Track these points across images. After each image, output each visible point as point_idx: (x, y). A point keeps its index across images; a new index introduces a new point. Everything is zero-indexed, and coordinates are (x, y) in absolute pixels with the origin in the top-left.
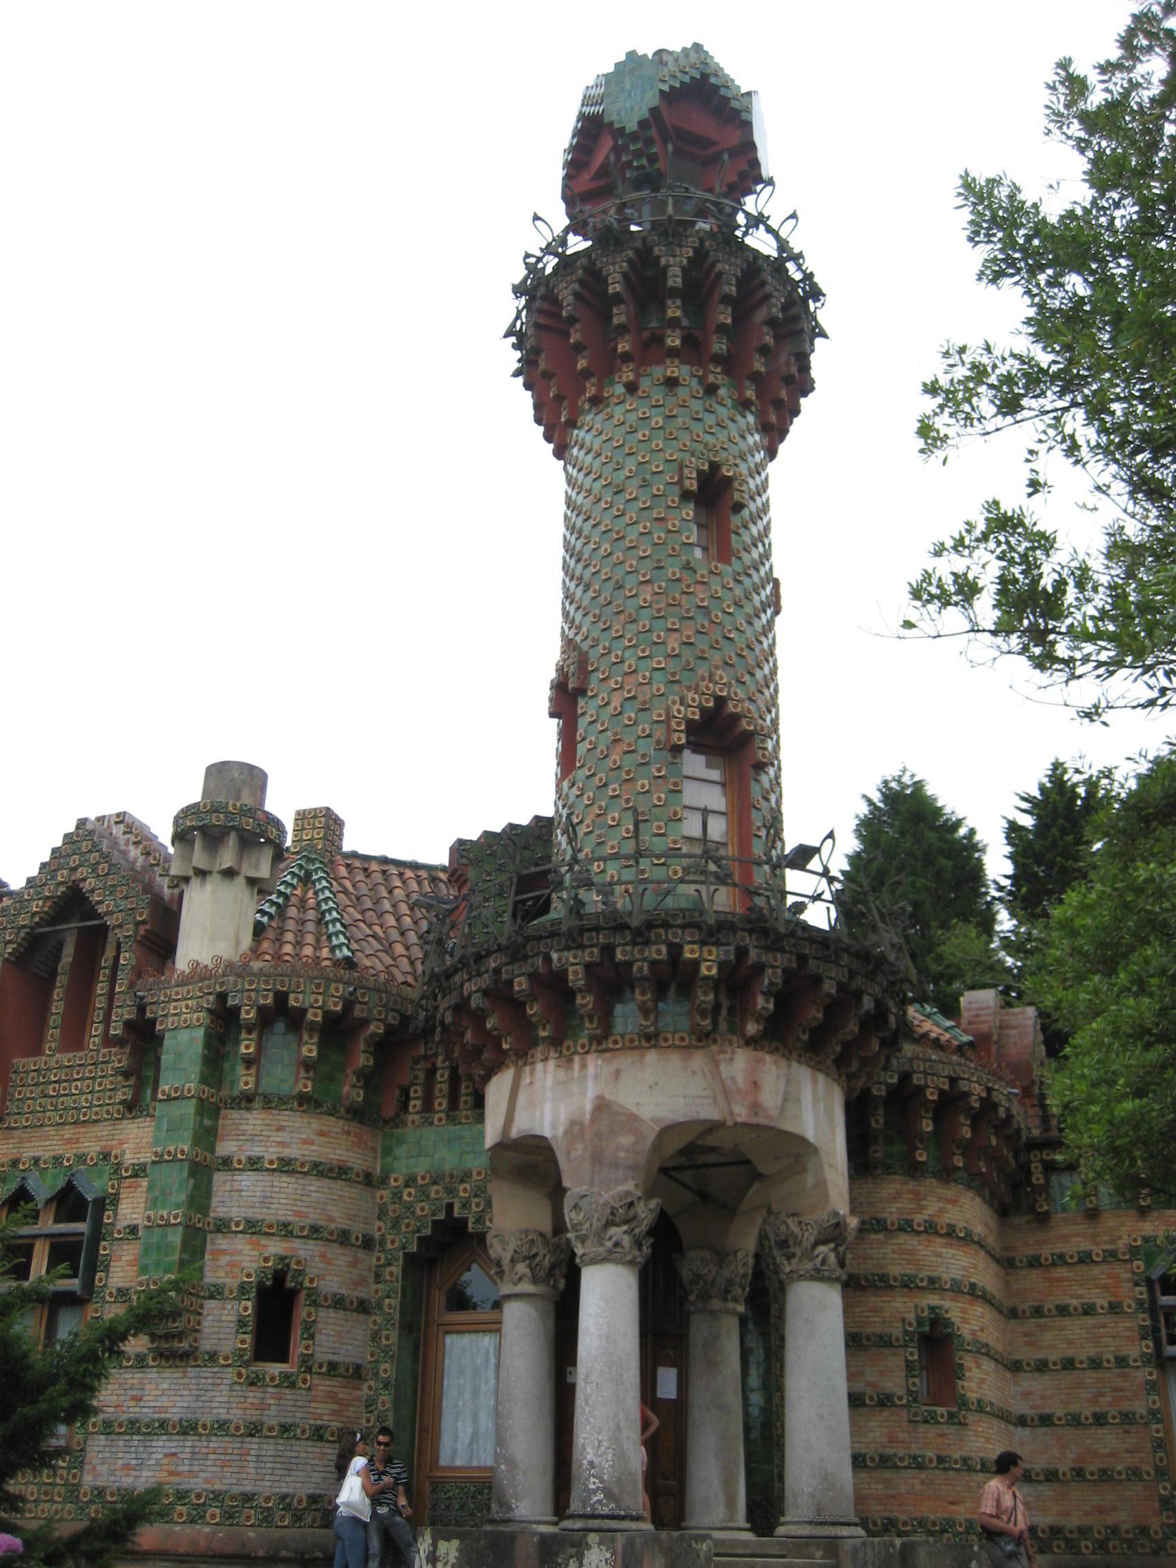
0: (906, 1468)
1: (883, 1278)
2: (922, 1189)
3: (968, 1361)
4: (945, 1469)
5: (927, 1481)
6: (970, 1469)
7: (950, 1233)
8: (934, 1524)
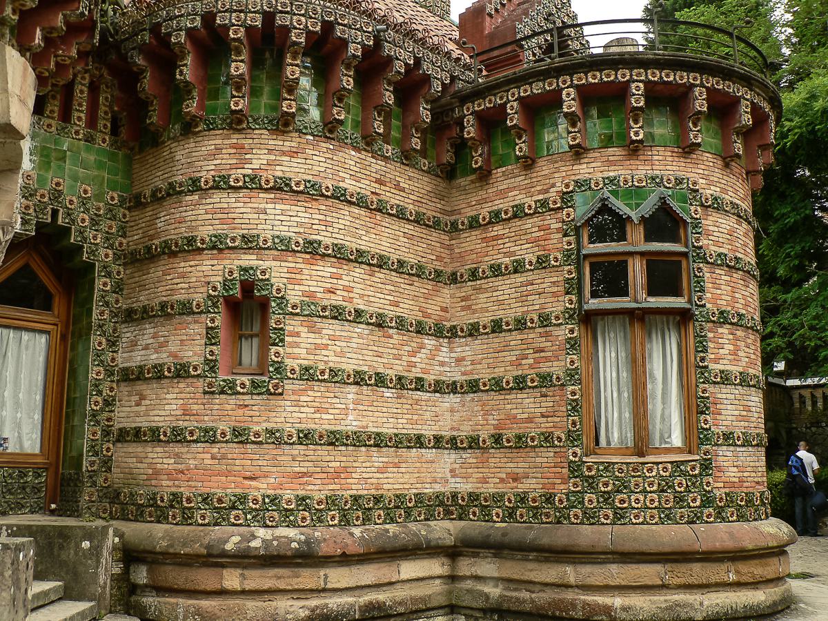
0: (194, 441)
1: (191, 241)
2: (247, 142)
3: (291, 325)
4: (241, 442)
5: (219, 456)
6: (279, 442)
7: (282, 187)
8: (220, 501)
